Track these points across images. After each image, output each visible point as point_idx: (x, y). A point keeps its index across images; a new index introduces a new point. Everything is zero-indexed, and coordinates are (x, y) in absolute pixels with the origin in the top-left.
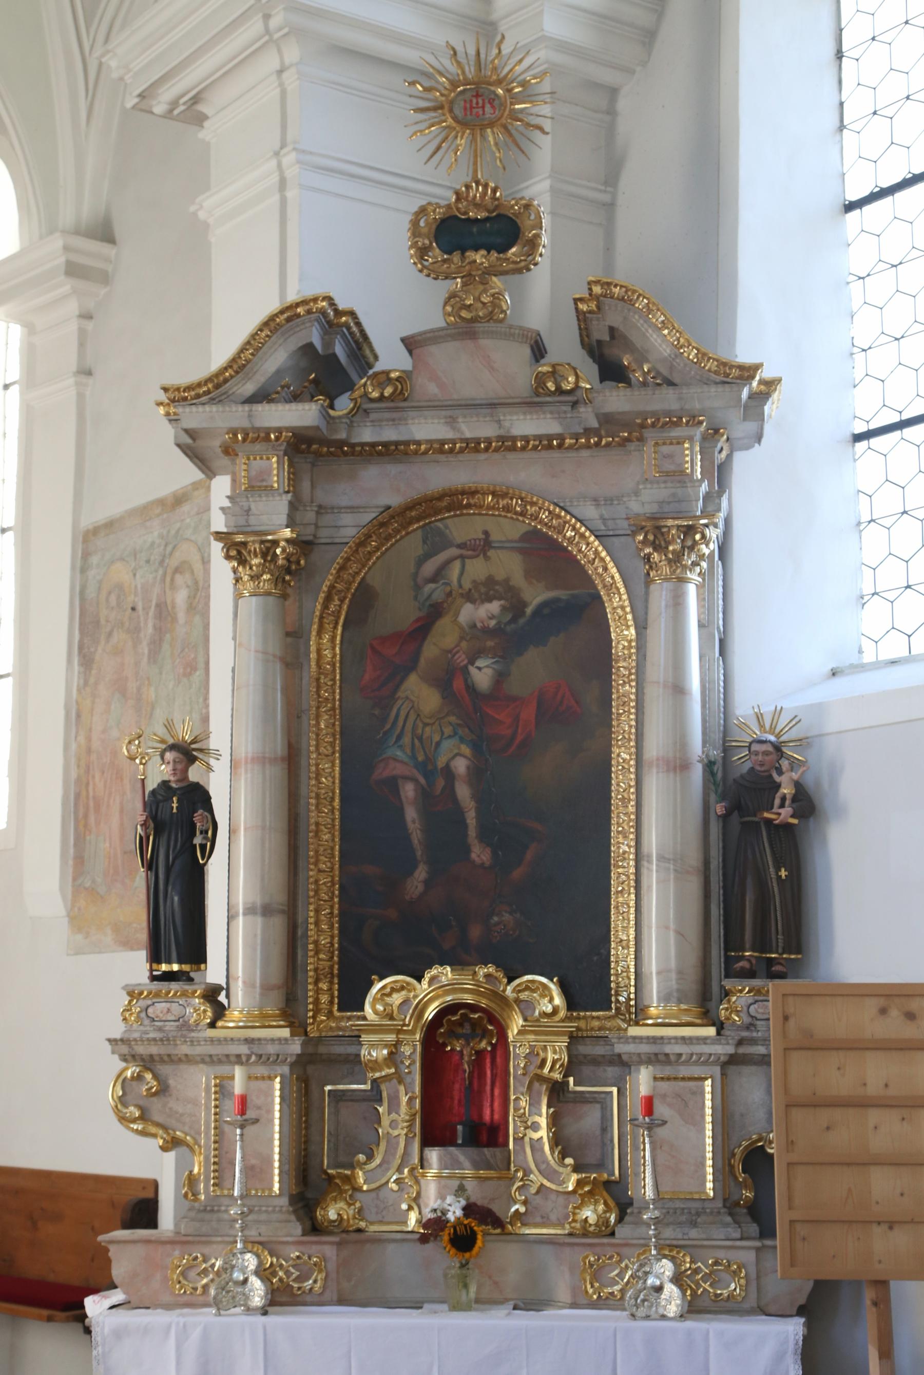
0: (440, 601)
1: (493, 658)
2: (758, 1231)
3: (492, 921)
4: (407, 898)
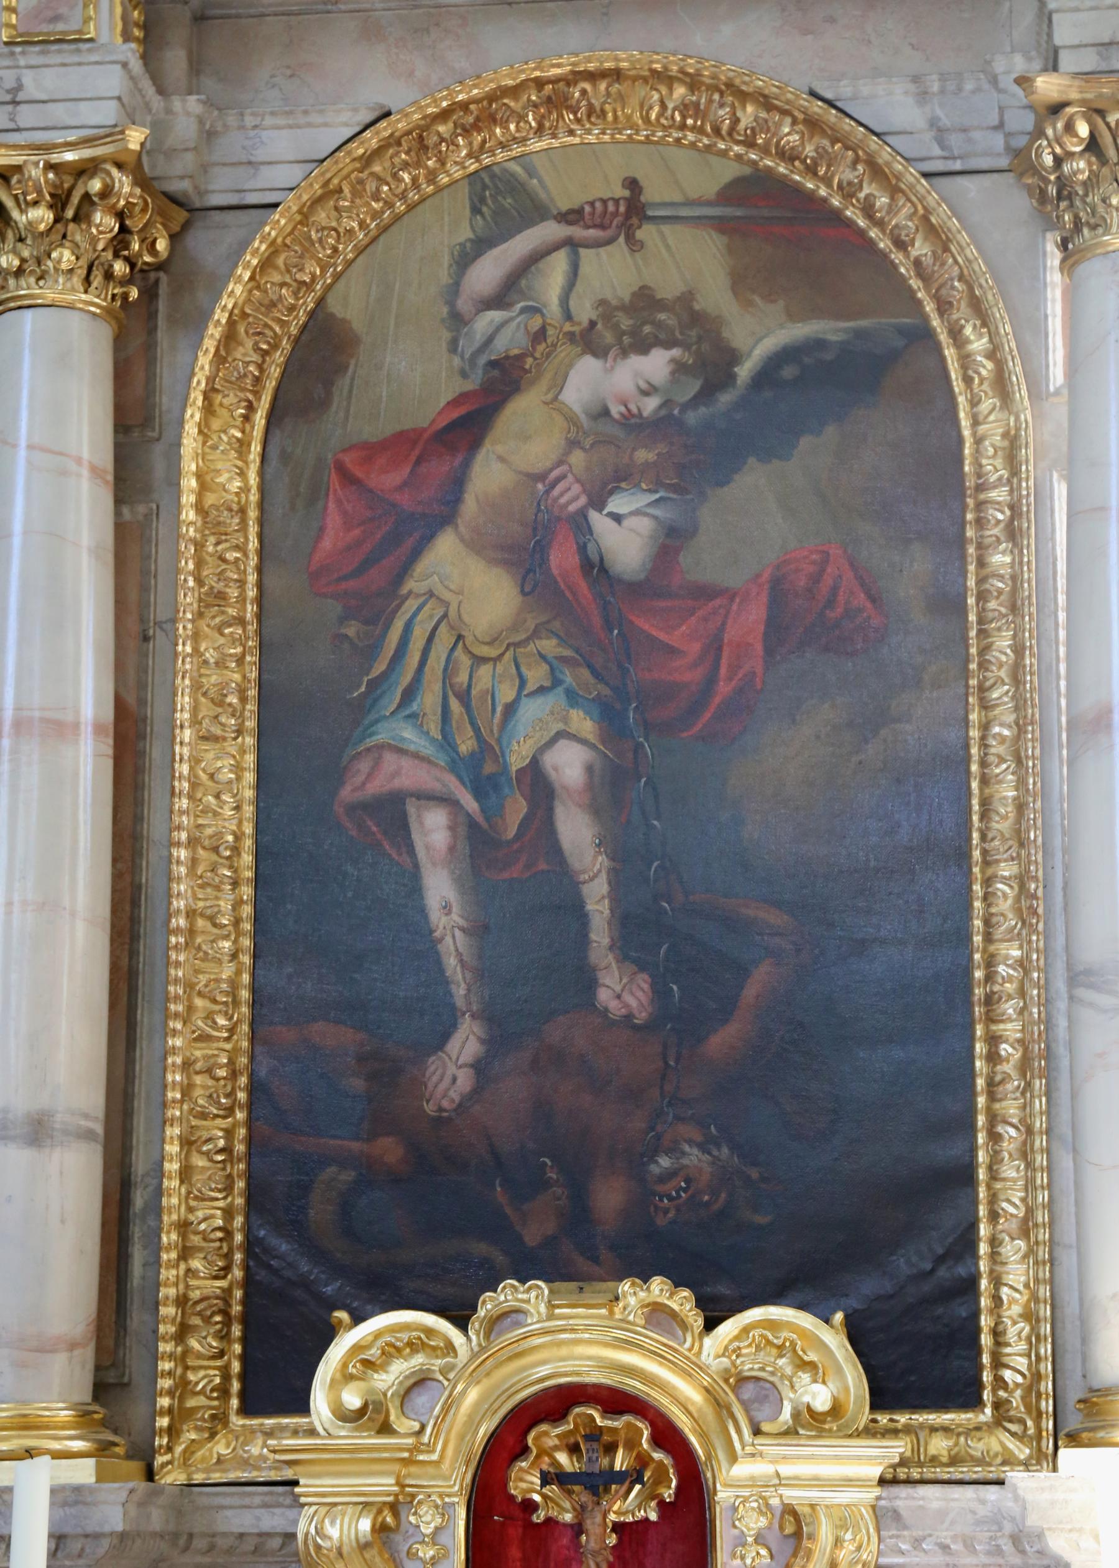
0: (516, 352)
1: (650, 491)
3: (654, 1169)
4: (430, 1108)
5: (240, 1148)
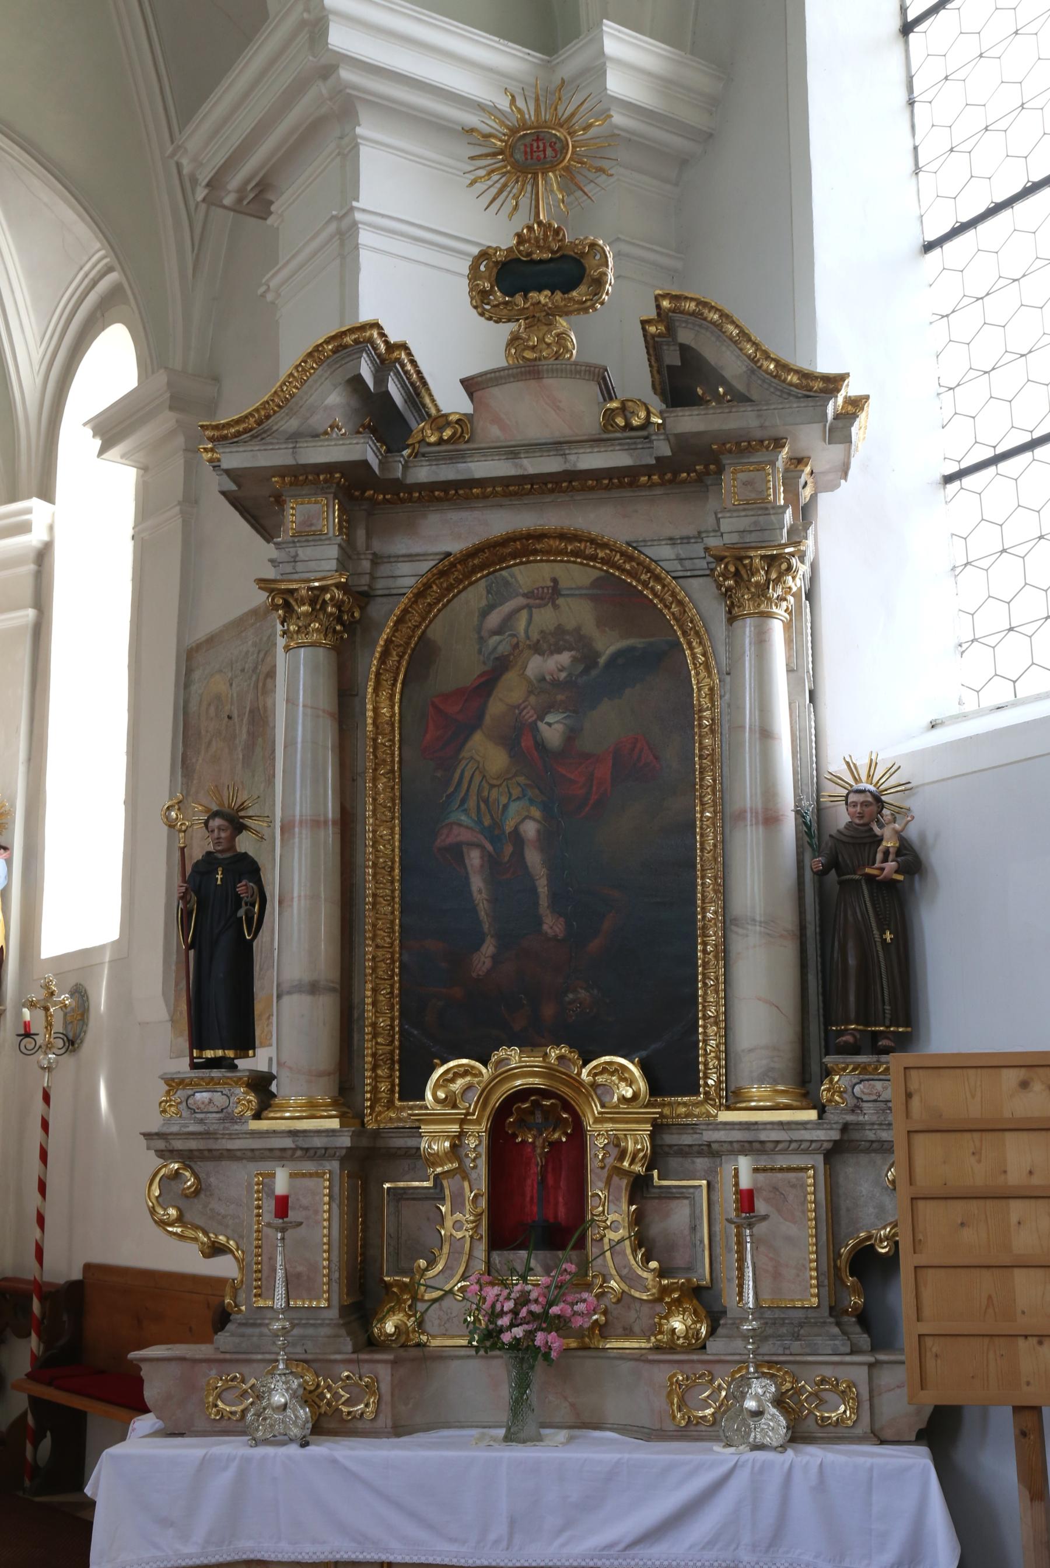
2: (869, 1344)
3: (567, 999)
4: (474, 975)
5: (396, 992)
